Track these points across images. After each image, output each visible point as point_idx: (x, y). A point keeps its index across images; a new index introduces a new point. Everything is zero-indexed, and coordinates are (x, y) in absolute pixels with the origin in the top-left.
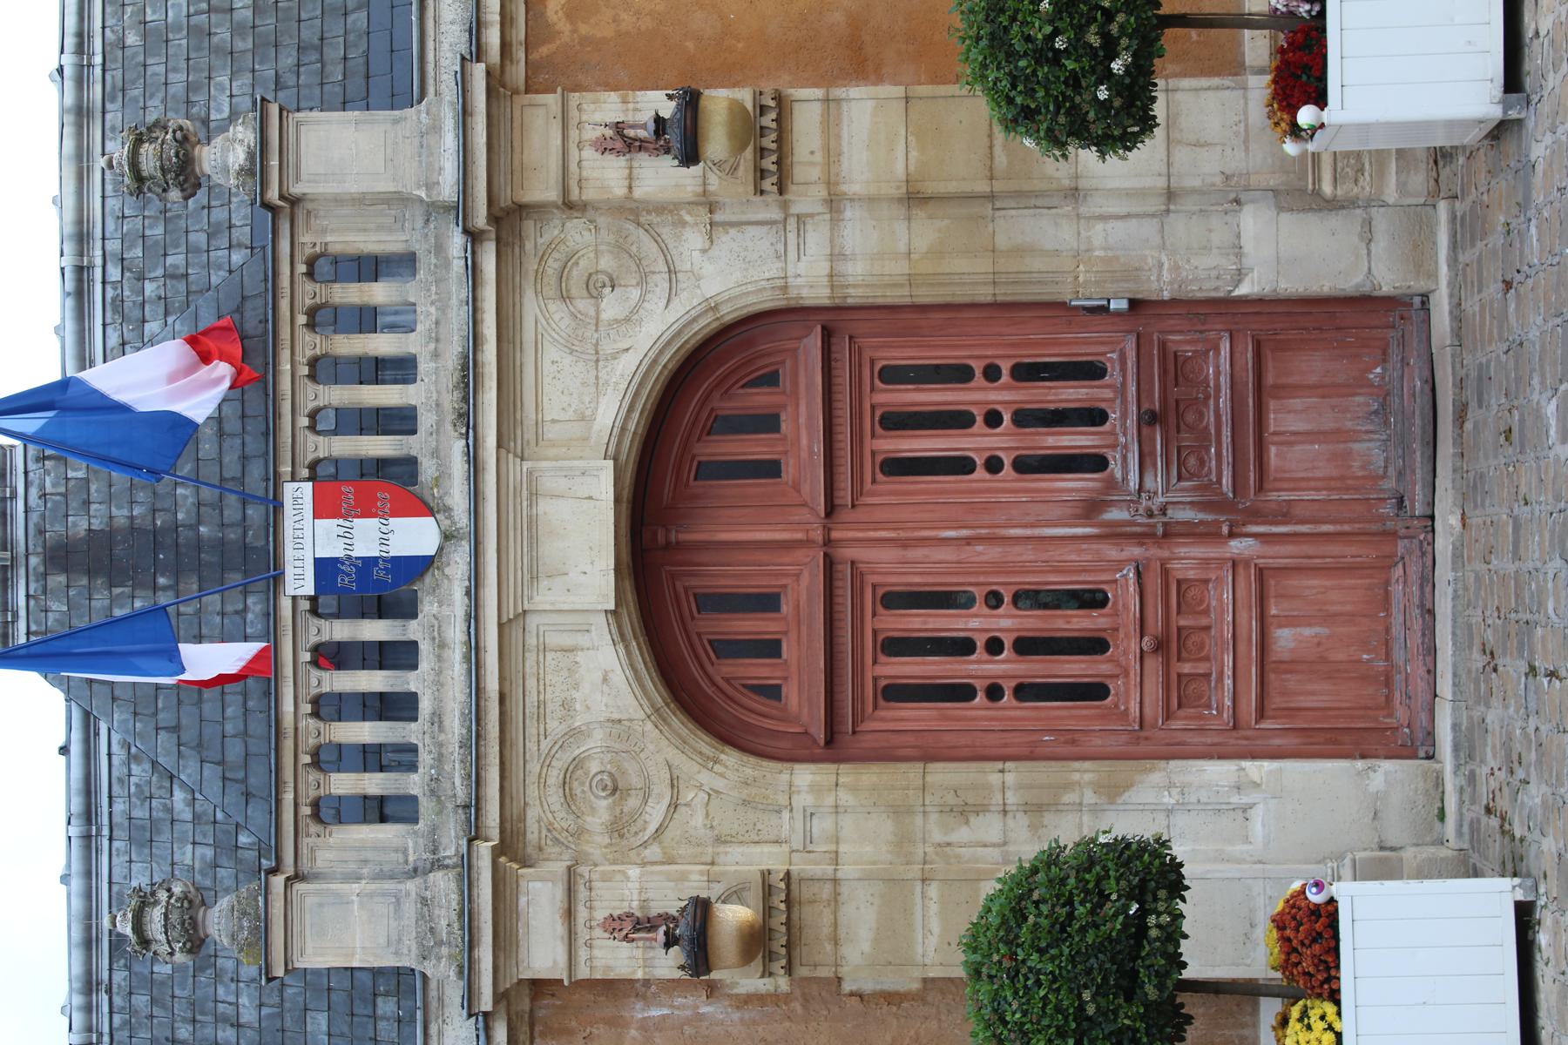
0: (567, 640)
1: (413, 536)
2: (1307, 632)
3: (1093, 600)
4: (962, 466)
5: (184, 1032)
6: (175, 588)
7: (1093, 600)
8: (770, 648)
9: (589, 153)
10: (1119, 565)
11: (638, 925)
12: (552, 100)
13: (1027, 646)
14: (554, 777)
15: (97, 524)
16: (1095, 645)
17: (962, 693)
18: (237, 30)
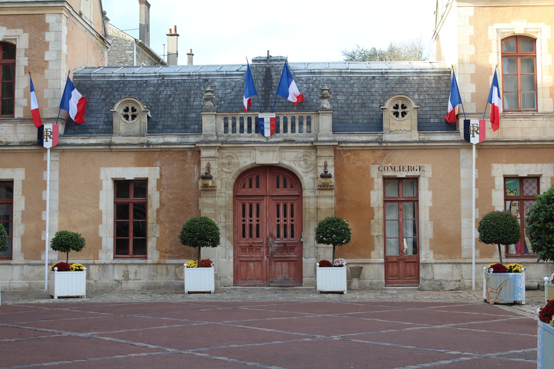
0: (251, 156)
1: (267, 133)
3: (258, 236)
4: (278, 216)
5: (192, 92)
6: (262, 91)
7: (258, 236)
8: (251, 187)
9: (325, 160)
10: (263, 240)
11: (208, 168)
12: (333, 154)
13: (251, 226)
14: (231, 154)
15: (273, 77)
16: (251, 236)
17: (244, 216)
18: (351, 100)
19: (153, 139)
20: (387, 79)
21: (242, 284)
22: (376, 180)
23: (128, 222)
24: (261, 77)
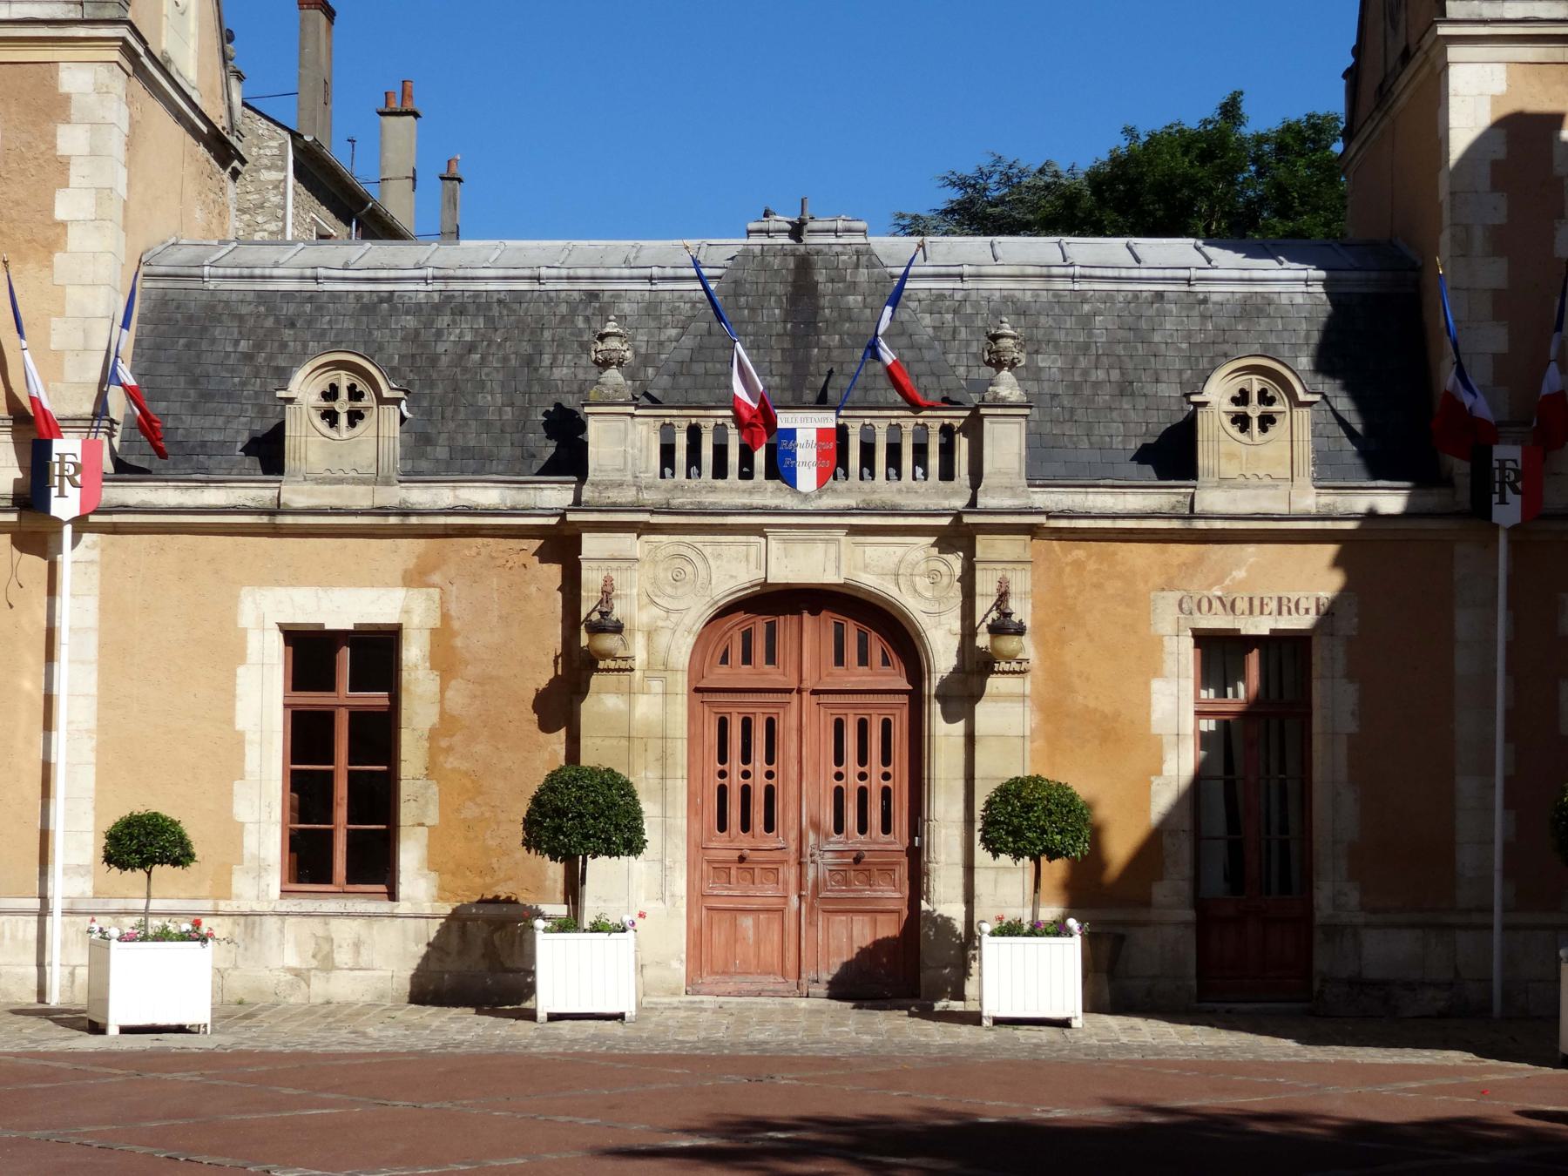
0: (753, 558)
1: (807, 478)
2: (751, 933)
3: (769, 826)
4: (839, 759)
5: (547, 335)
6: (785, 334)
7: (769, 826)
8: (747, 659)
9: (1000, 574)
11: (607, 595)
13: (746, 792)
15: (821, 287)
16: (746, 826)
17: (723, 758)
18: (1085, 372)
19: (419, 496)
20: (1205, 301)
21: (716, 989)
22: (1170, 644)
23: (331, 773)
24: (779, 289)
